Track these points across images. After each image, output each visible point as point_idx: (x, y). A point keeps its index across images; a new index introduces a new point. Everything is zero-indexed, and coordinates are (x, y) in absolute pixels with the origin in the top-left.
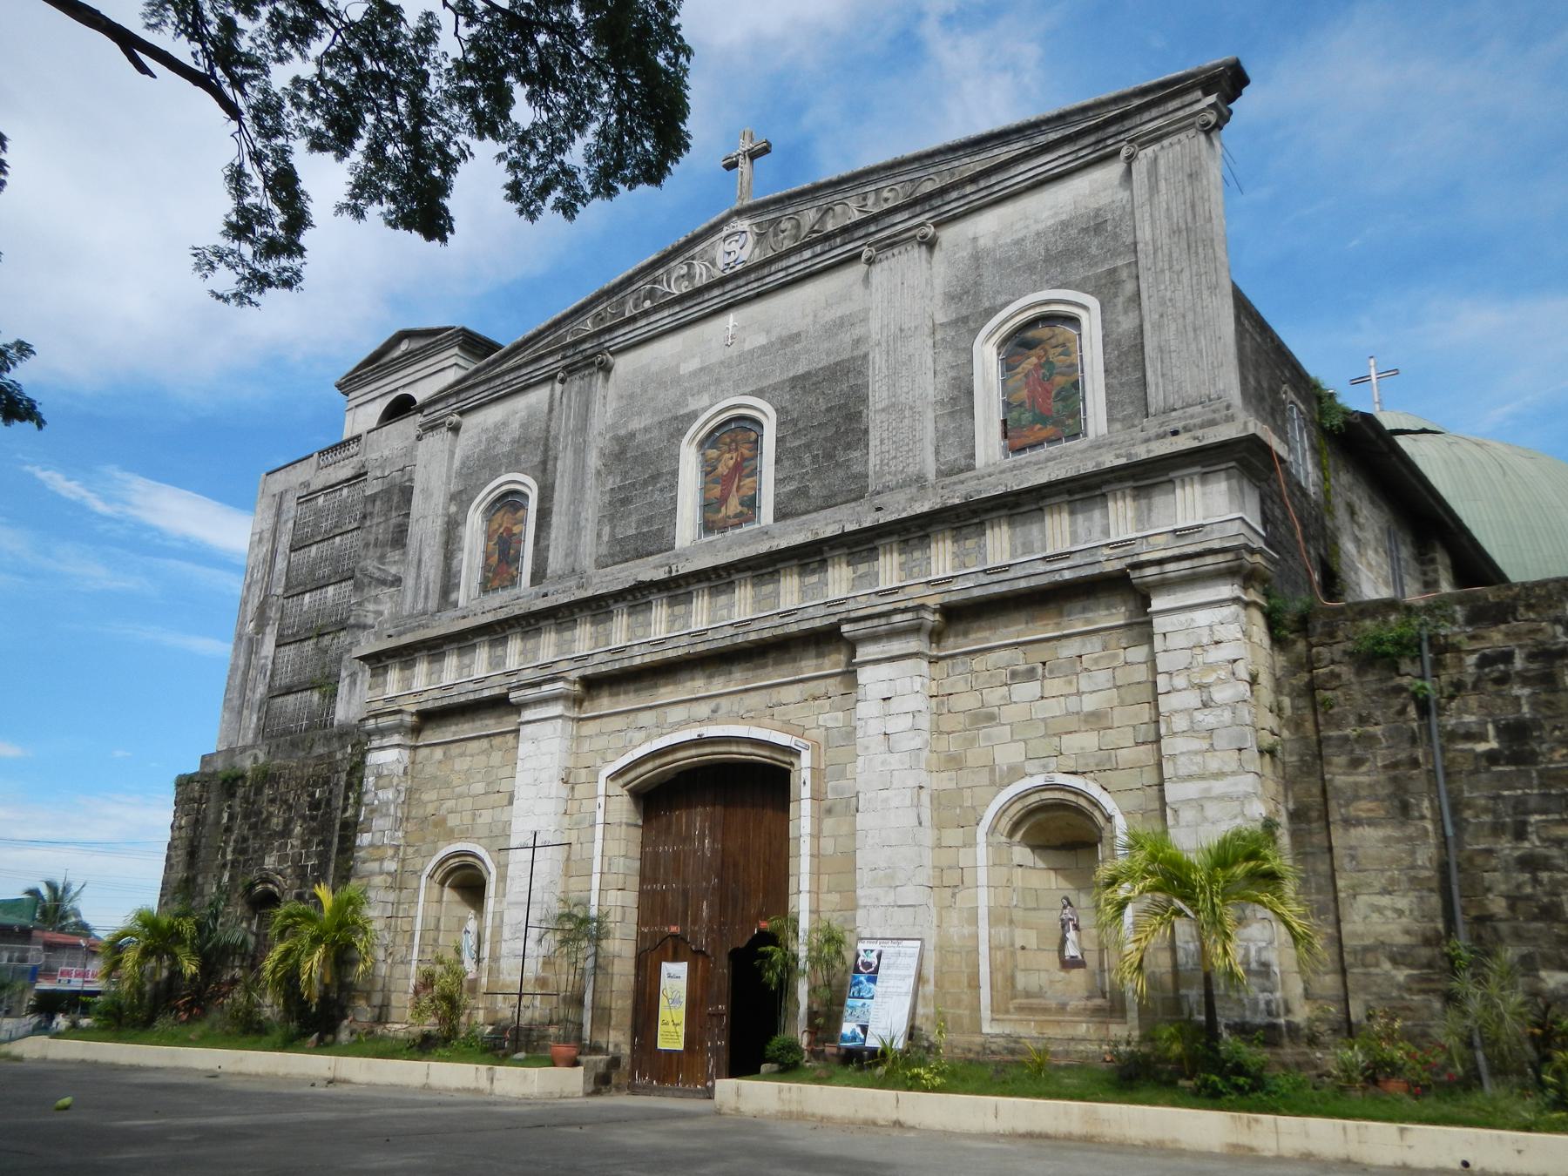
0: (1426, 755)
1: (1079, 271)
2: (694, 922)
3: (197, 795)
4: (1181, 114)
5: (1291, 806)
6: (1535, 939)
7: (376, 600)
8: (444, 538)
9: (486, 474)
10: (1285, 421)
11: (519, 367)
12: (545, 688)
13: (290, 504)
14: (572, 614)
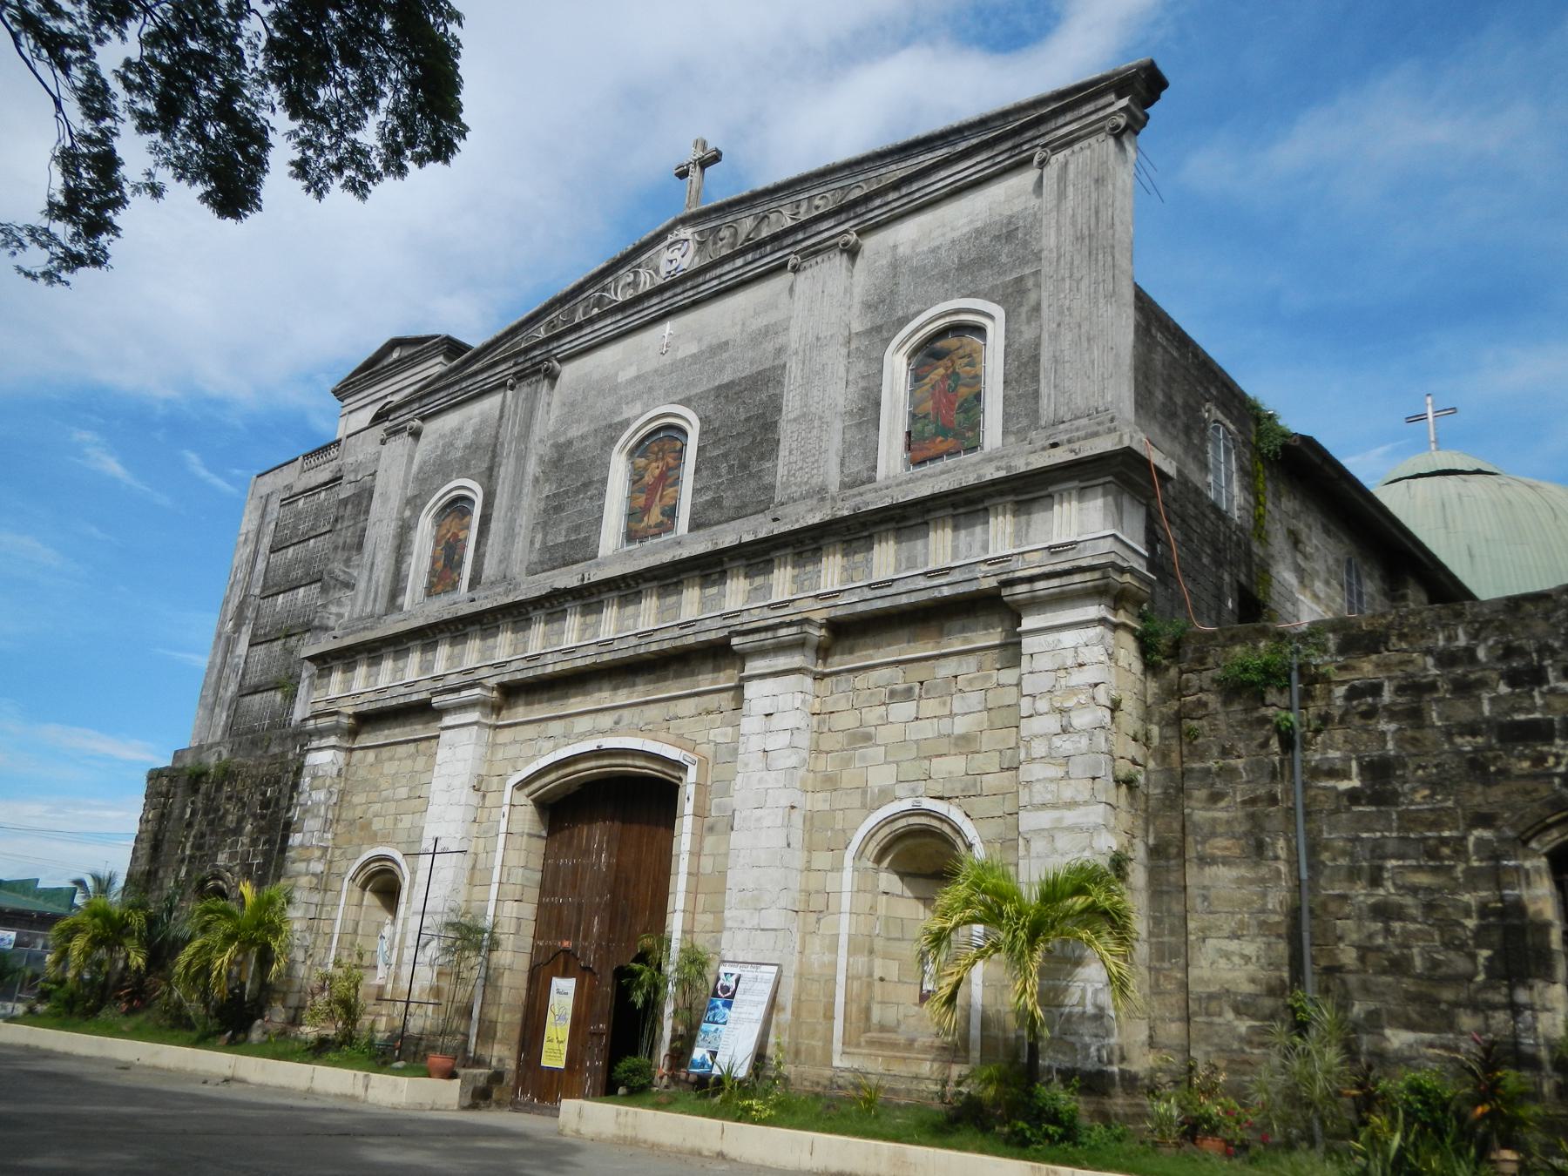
0: (1286, 792)
1: (987, 279)
2: (585, 939)
3: (164, 789)
4: (1094, 117)
5: (1151, 841)
6: (1383, 994)
7: (339, 603)
8: (396, 543)
9: (438, 479)
10: (1204, 440)
11: (476, 373)
12: (464, 693)
13: (274, 505)
14: (496, 620)
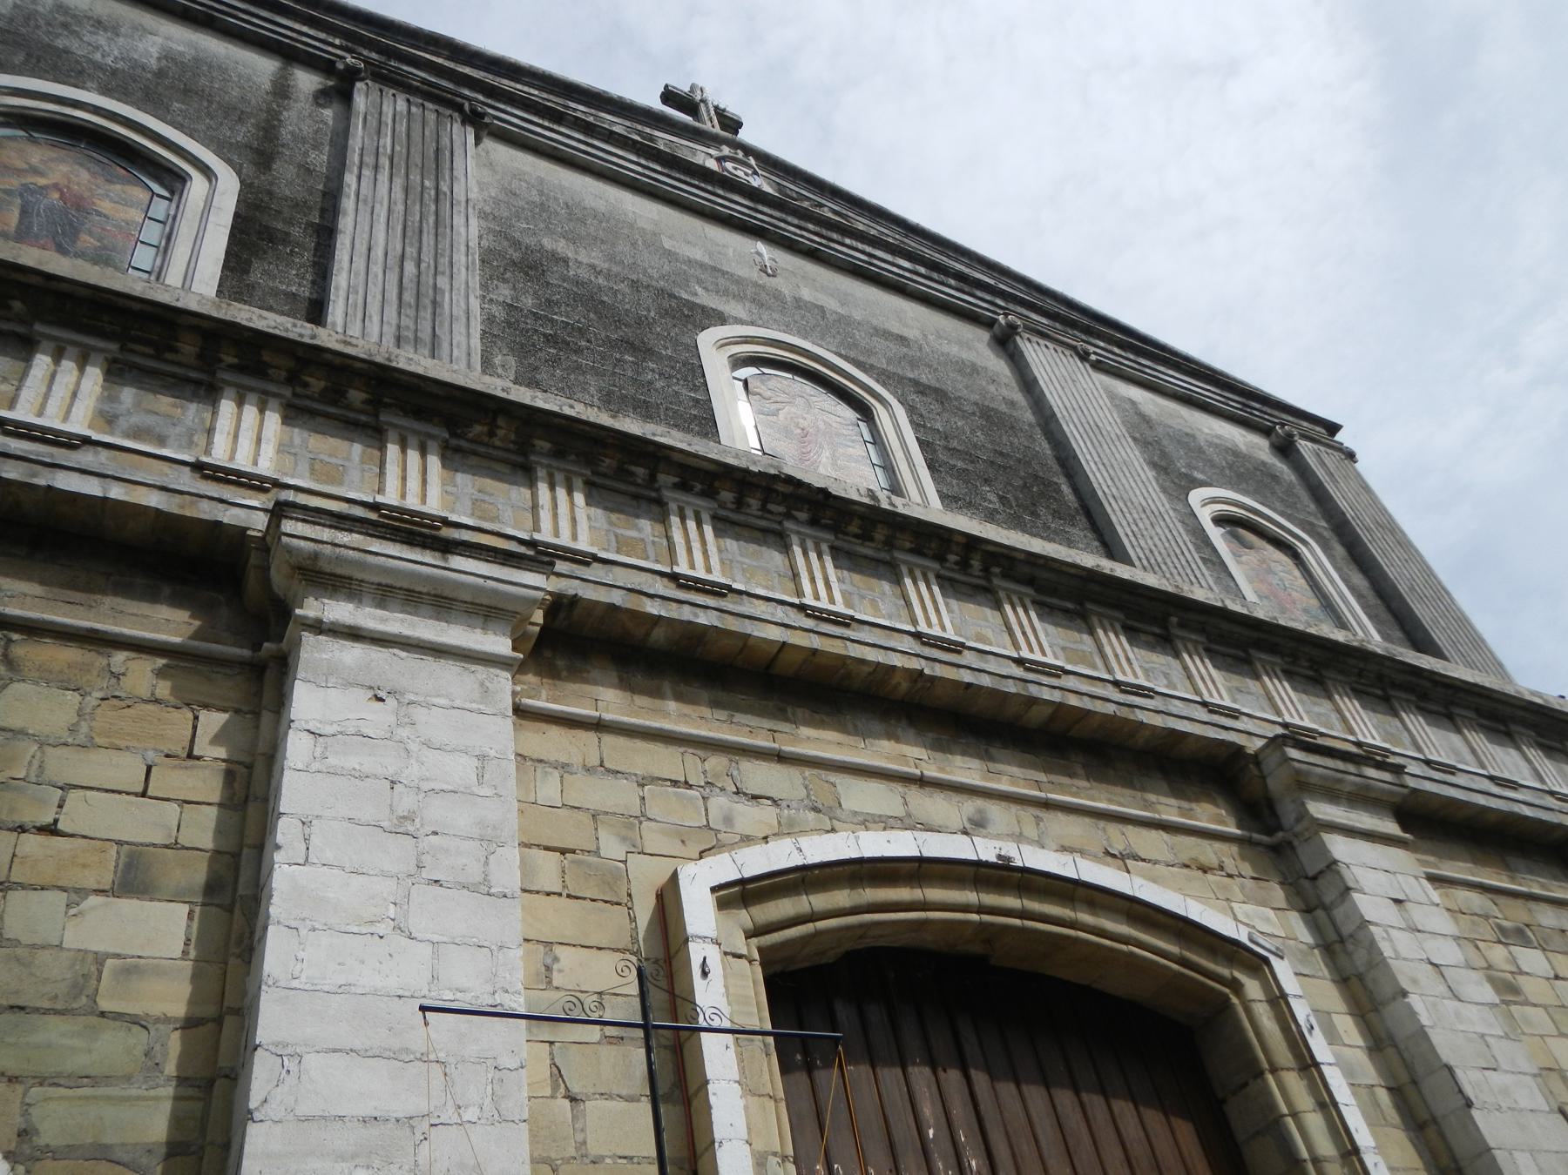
12: (458, 562)
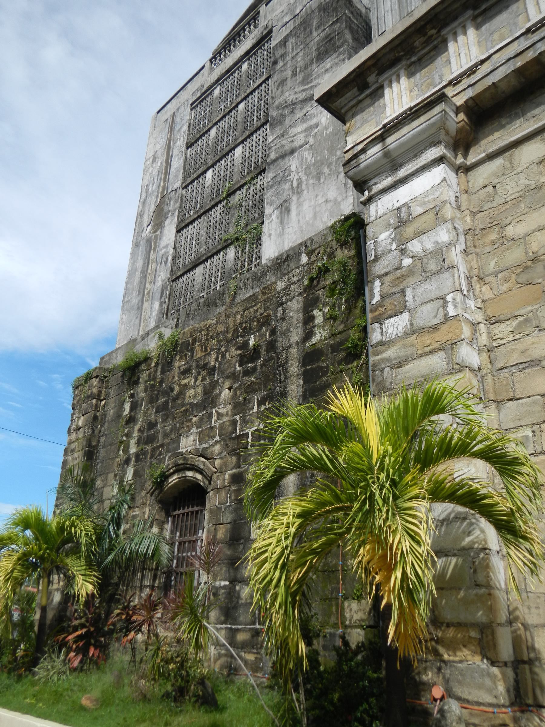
3: (95, 390)
